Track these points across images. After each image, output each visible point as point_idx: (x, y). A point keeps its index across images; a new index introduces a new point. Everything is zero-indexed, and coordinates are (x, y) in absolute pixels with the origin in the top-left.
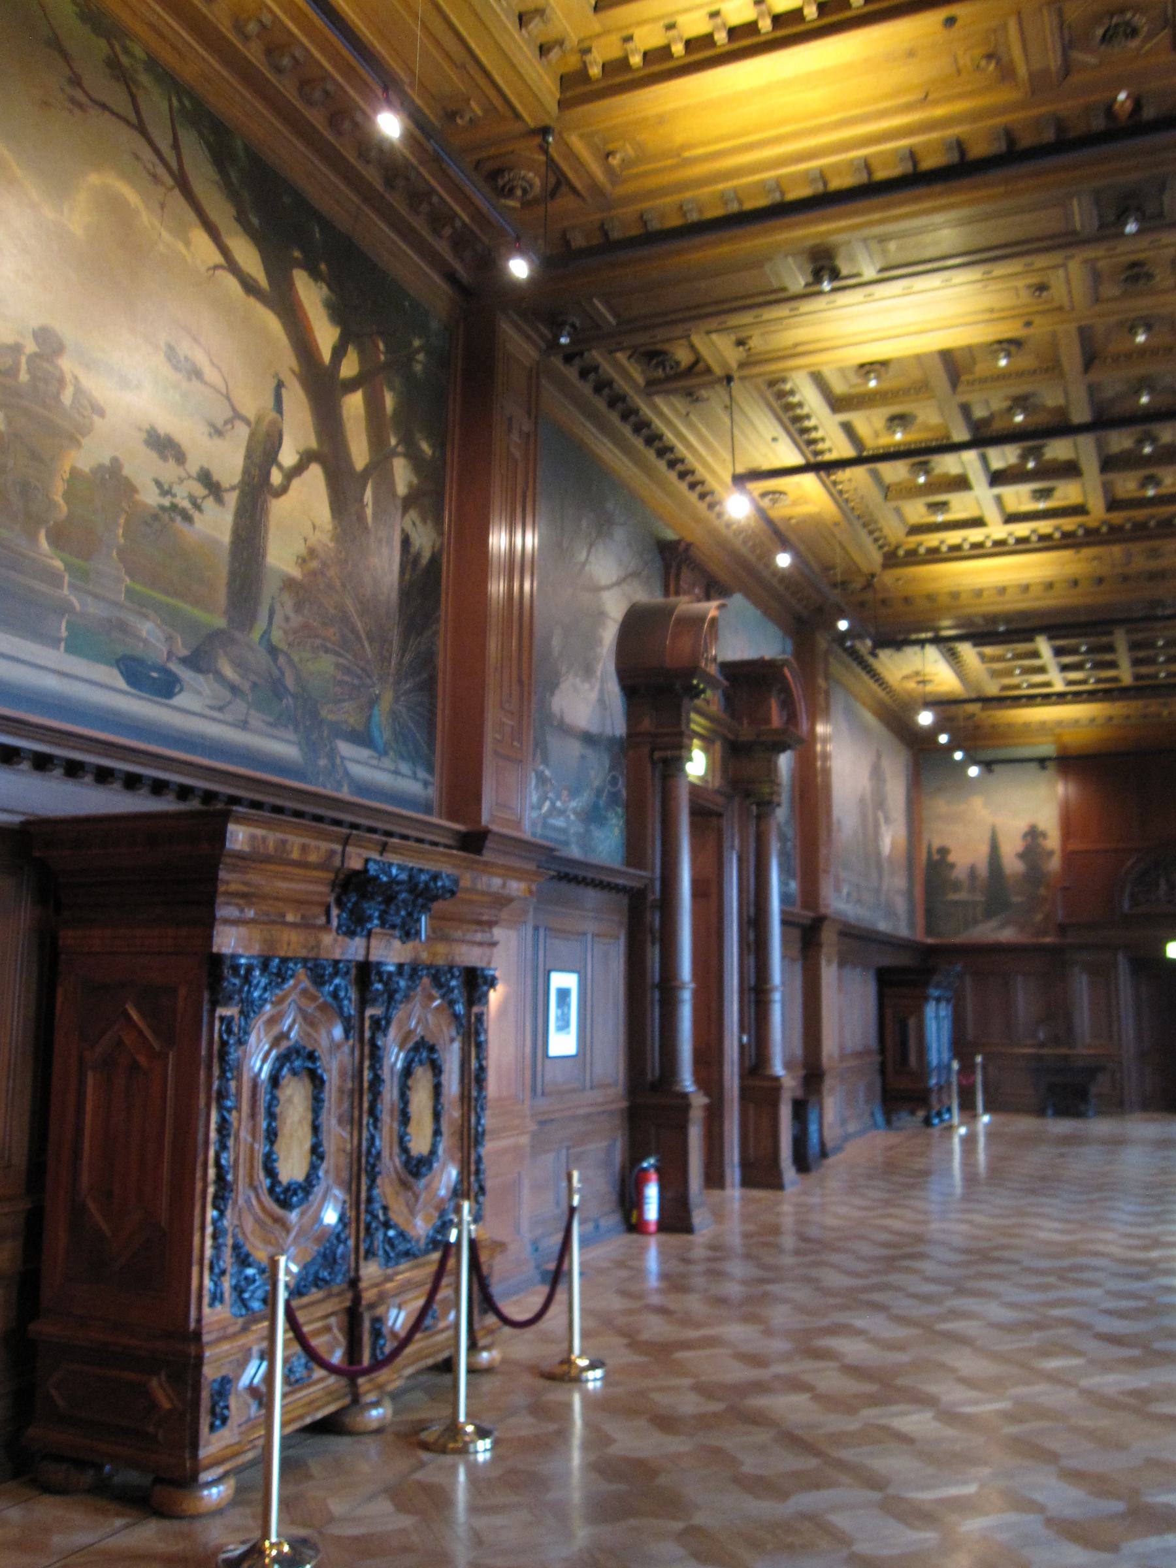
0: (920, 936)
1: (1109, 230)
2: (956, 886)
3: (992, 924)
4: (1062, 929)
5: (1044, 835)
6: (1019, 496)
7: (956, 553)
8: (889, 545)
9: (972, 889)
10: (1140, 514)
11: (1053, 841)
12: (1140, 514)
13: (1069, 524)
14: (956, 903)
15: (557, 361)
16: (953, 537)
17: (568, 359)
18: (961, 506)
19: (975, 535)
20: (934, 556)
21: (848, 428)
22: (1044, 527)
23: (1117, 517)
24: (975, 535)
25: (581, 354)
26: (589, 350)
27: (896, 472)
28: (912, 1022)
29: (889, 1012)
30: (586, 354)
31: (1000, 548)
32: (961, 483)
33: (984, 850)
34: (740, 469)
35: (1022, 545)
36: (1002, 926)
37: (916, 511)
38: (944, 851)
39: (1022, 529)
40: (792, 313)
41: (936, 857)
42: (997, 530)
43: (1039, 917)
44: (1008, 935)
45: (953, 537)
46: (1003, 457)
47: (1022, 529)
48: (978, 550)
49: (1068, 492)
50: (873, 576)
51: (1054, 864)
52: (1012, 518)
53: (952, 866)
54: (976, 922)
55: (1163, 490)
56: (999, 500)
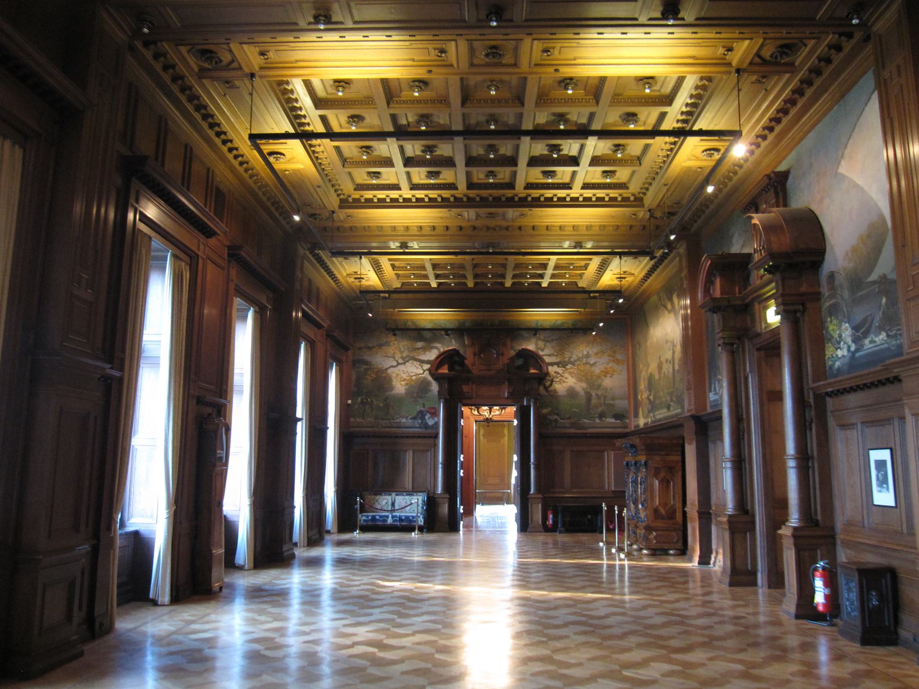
1: (481, 24)
6: (419, 175)
7: (382, 204)
8: (344, 194)
10: (484, 193)
12: (484, 193)
13: (446, 194)
15: (139, 45)
16: (381, 194)
17: (146, 44)
18: (389, 175)
19: (394, 194)
20: (370, 204)
21: (324, 119)
22: (433, 194)
23: (472, 193)
24: (394, 194)
25: (155, 43)
26: (161, 41)
27: (350, 148)
30: (159, 44)
31: (407, 203)
32: (388, 163)
34: (254, 132)
35: (419, 204)
37: (361, 175)
39: (420, 194)
40: (296, 40)
42: (407, 193)
45: (381, 194)
46: (413, 148)
47: (420, 194)
48: (394, 204)
49: (447, 175)
50: (333, 212)
52: (414, 187)
55: (497, 181)
56: (408, 174)
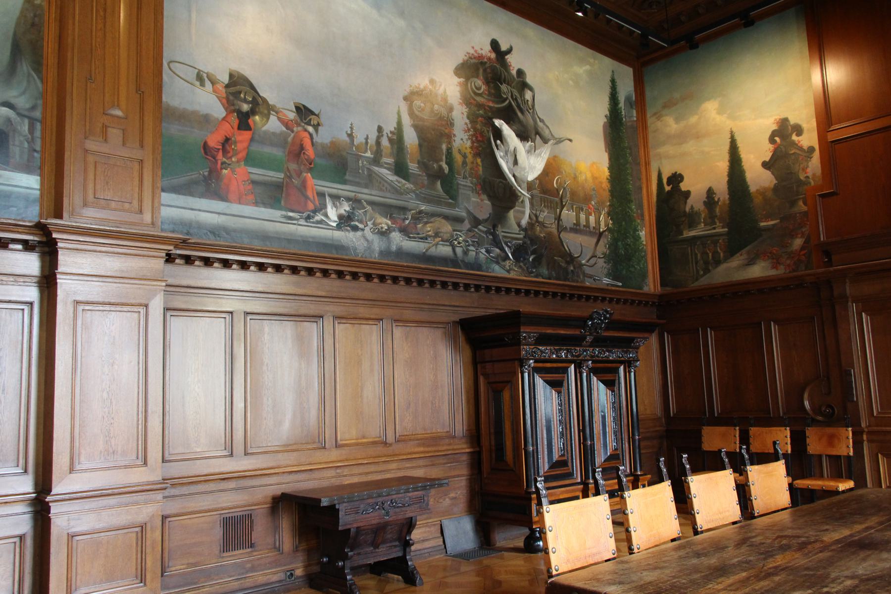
0: (652, 285)
2: (692, 219)
3: (736, 261)
4: (827, 252)
5: (799, 130)
9: (711, 219)
11: (809, 139)
14: (694, 238)
28: (506, 395)
29: (482, 380)
33: (723, 165)
36: (750, 262)
38: (676, 179)
41: (667, 188)
43: (798, 242)
44: (759, 271)
51: (815, 164)
53: (687, 194)
54: (718, 263)
